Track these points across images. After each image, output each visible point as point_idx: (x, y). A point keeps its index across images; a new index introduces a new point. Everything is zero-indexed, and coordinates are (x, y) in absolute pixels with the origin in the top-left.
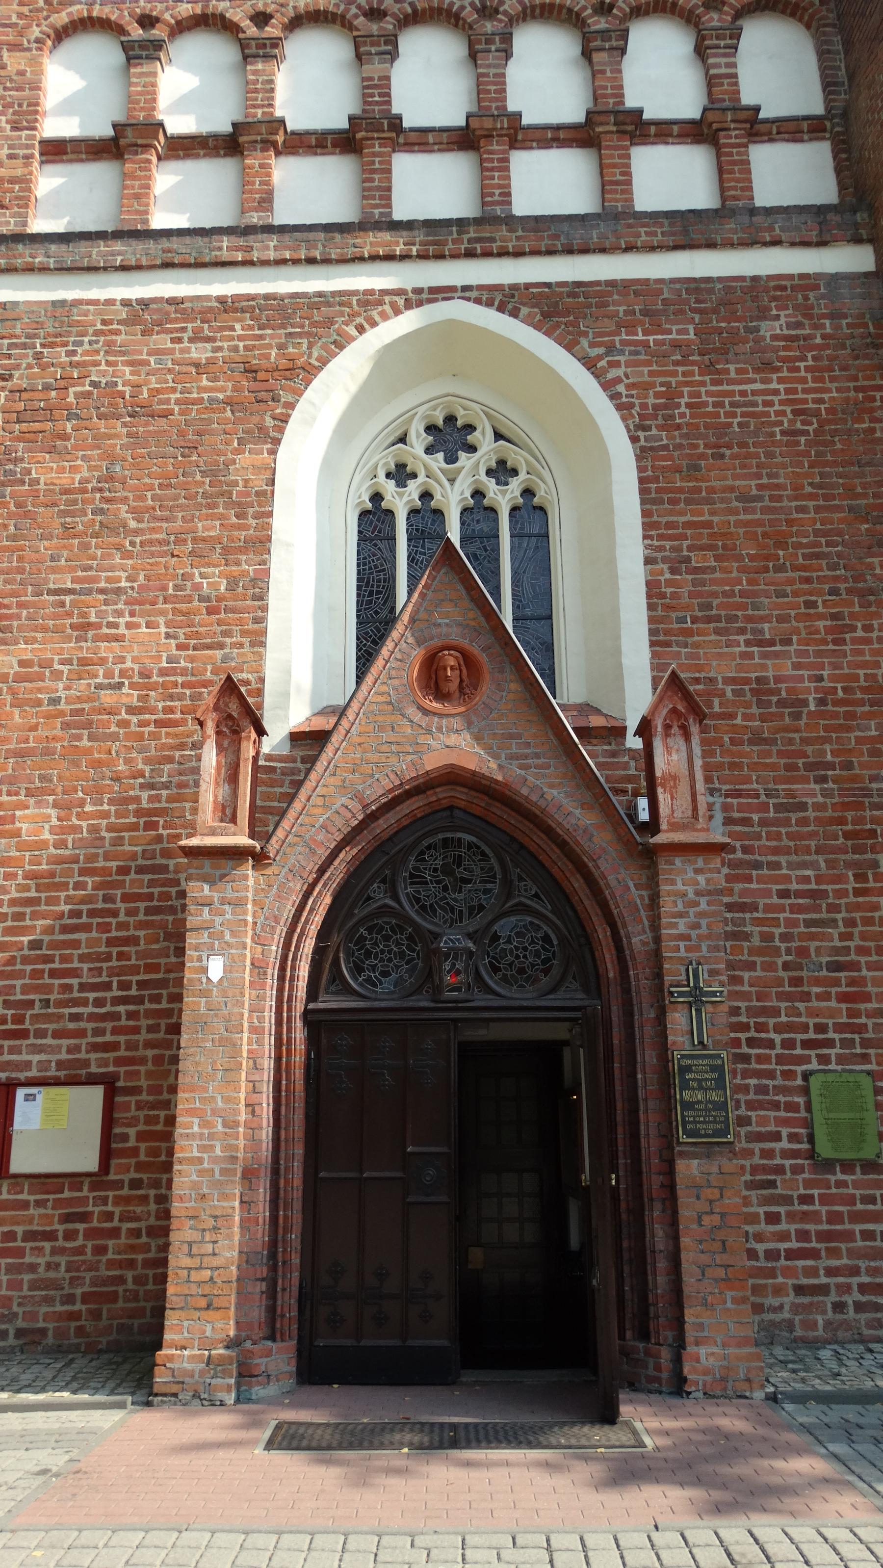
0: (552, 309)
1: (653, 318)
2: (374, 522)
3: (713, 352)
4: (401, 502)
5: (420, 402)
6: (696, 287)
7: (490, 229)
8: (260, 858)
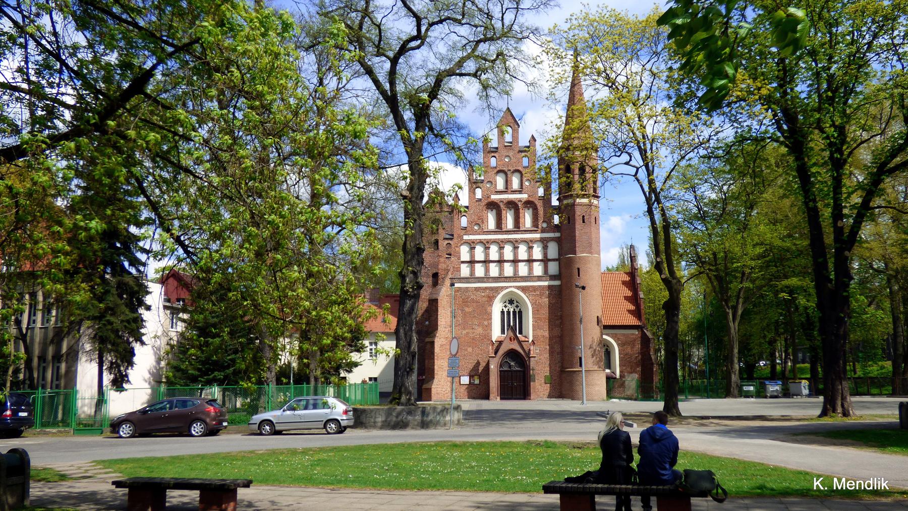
0: (523, 289)
1: (535, 291)
2: (503, 312)
3: (541, 295)
4: (506, 310)
5: (508, 298)
6: (540, 286)
7: (515, 278)
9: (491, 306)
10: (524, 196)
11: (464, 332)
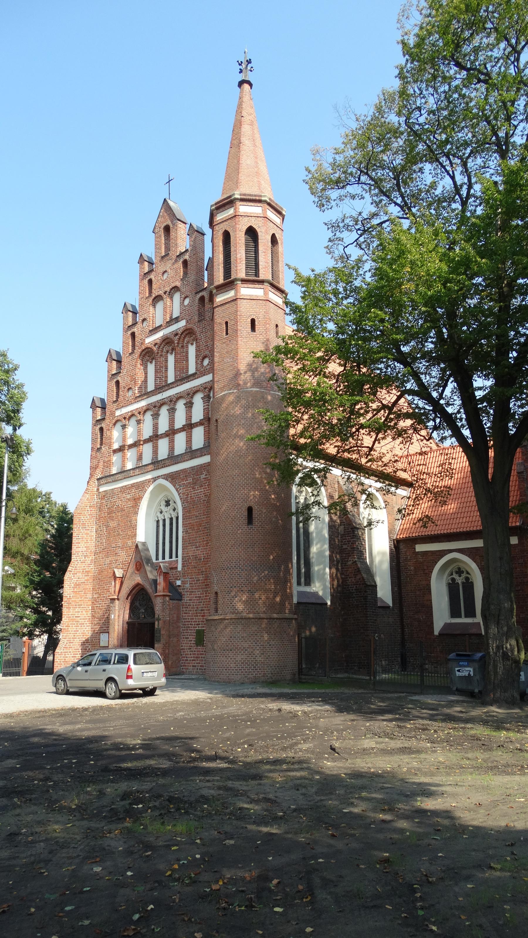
4: (161, 517)
5: (161, 498)
6: (192, 468)
8: (118, 599)
9: (136, 513)
10: (182, 324)
11: (108, 561)
